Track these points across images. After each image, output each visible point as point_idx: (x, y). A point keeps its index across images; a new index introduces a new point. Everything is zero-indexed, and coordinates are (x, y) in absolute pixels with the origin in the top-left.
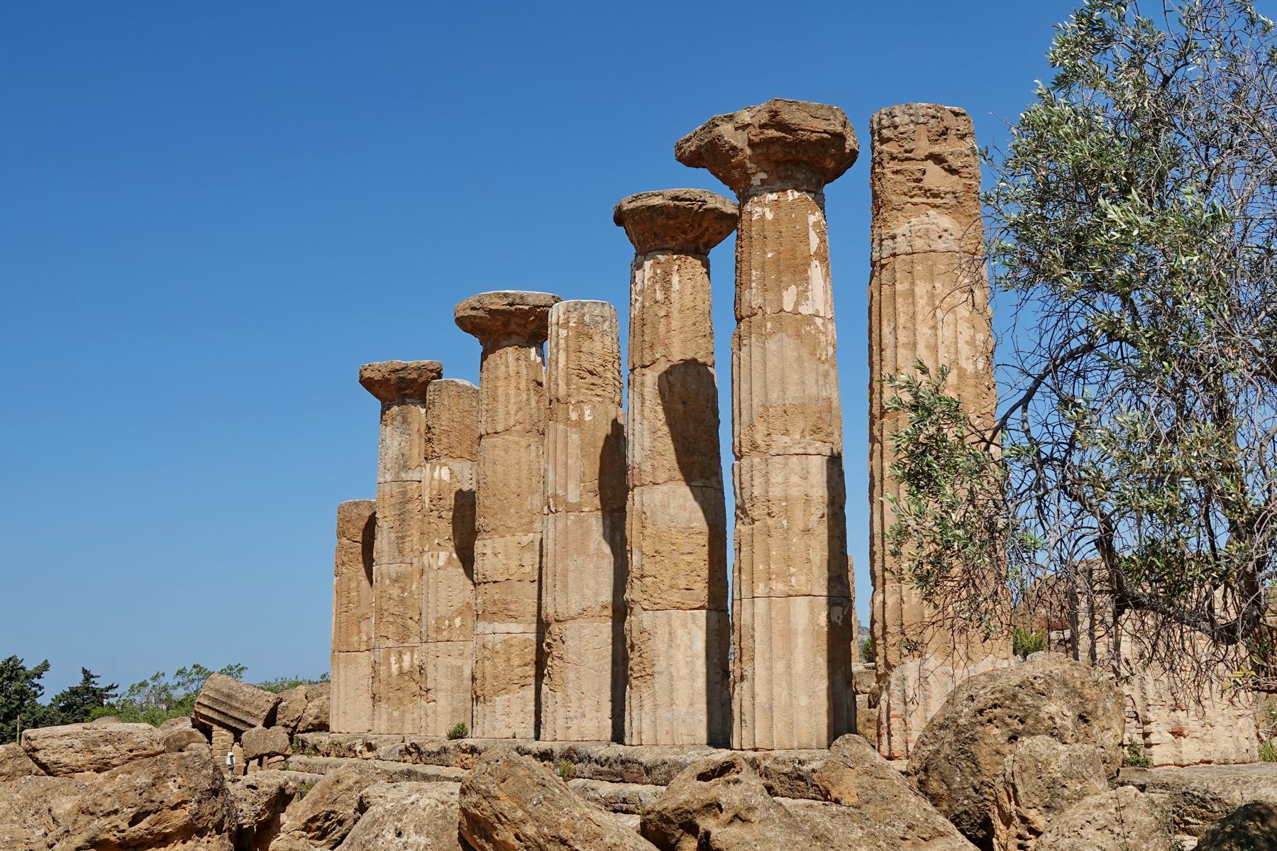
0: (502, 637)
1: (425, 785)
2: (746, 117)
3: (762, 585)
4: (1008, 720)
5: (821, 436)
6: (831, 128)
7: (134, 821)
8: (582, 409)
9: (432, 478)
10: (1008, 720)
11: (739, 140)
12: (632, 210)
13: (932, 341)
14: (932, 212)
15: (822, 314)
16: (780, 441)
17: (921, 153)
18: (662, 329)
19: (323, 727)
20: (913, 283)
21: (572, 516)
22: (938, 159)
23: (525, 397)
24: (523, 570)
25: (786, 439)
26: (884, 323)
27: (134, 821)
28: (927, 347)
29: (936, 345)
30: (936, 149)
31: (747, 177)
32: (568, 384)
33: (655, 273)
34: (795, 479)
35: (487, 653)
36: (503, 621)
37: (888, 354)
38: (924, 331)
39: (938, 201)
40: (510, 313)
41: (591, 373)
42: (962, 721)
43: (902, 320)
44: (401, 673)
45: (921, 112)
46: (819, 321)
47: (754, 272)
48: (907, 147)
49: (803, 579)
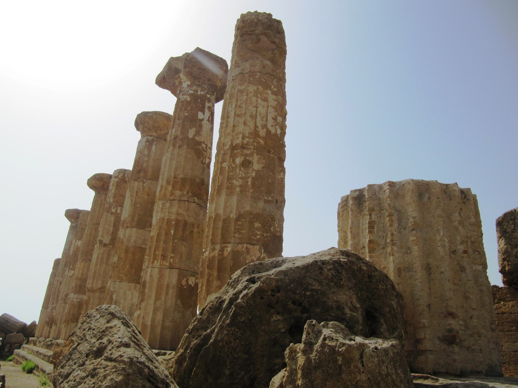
0: (78, 300)
3: (156, 262)
13: (254, 113)
16: (178, 193)
28: (251, 116)
29: (256, 115)
33: (146, 144)
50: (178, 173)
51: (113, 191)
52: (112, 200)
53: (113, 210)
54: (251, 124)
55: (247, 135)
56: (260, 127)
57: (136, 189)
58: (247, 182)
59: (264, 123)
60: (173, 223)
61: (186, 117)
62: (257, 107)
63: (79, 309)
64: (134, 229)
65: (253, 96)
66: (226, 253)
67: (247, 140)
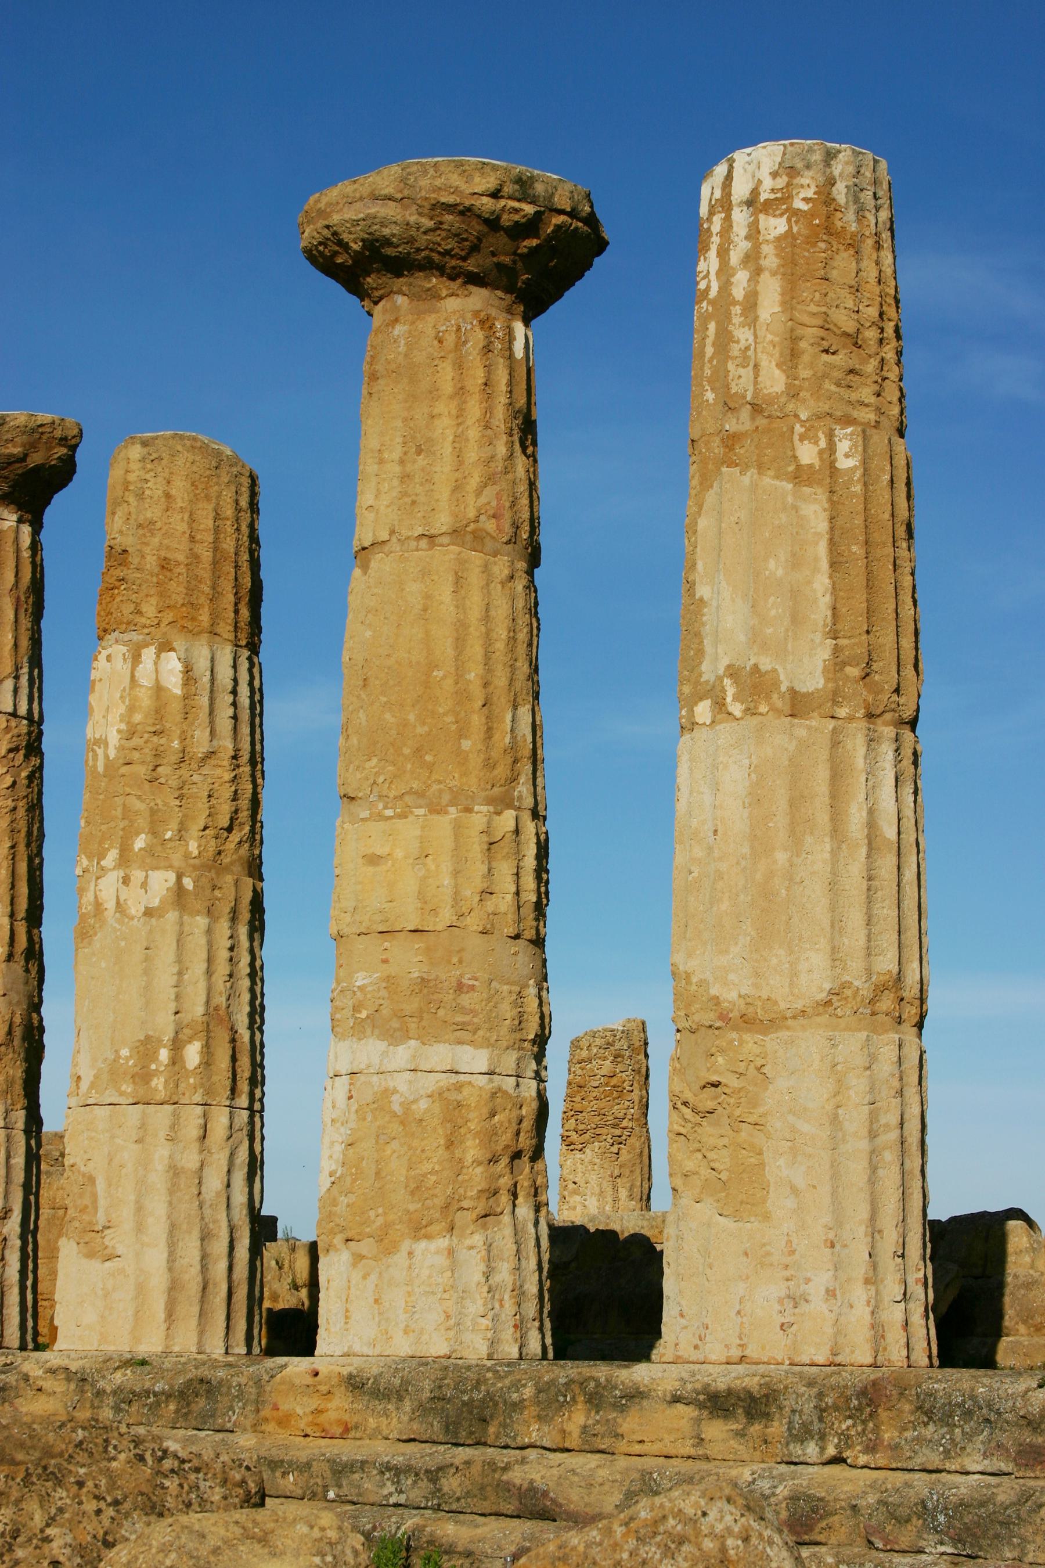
0: (431, 1083)
8: (830, 436)
21: (801, 729)
23: (502, 450)
24: (490, 905)
41: (855, 341)
51: (770, 306)
52: (774, 381)
53: (808, 454)
63: (450, 1145)
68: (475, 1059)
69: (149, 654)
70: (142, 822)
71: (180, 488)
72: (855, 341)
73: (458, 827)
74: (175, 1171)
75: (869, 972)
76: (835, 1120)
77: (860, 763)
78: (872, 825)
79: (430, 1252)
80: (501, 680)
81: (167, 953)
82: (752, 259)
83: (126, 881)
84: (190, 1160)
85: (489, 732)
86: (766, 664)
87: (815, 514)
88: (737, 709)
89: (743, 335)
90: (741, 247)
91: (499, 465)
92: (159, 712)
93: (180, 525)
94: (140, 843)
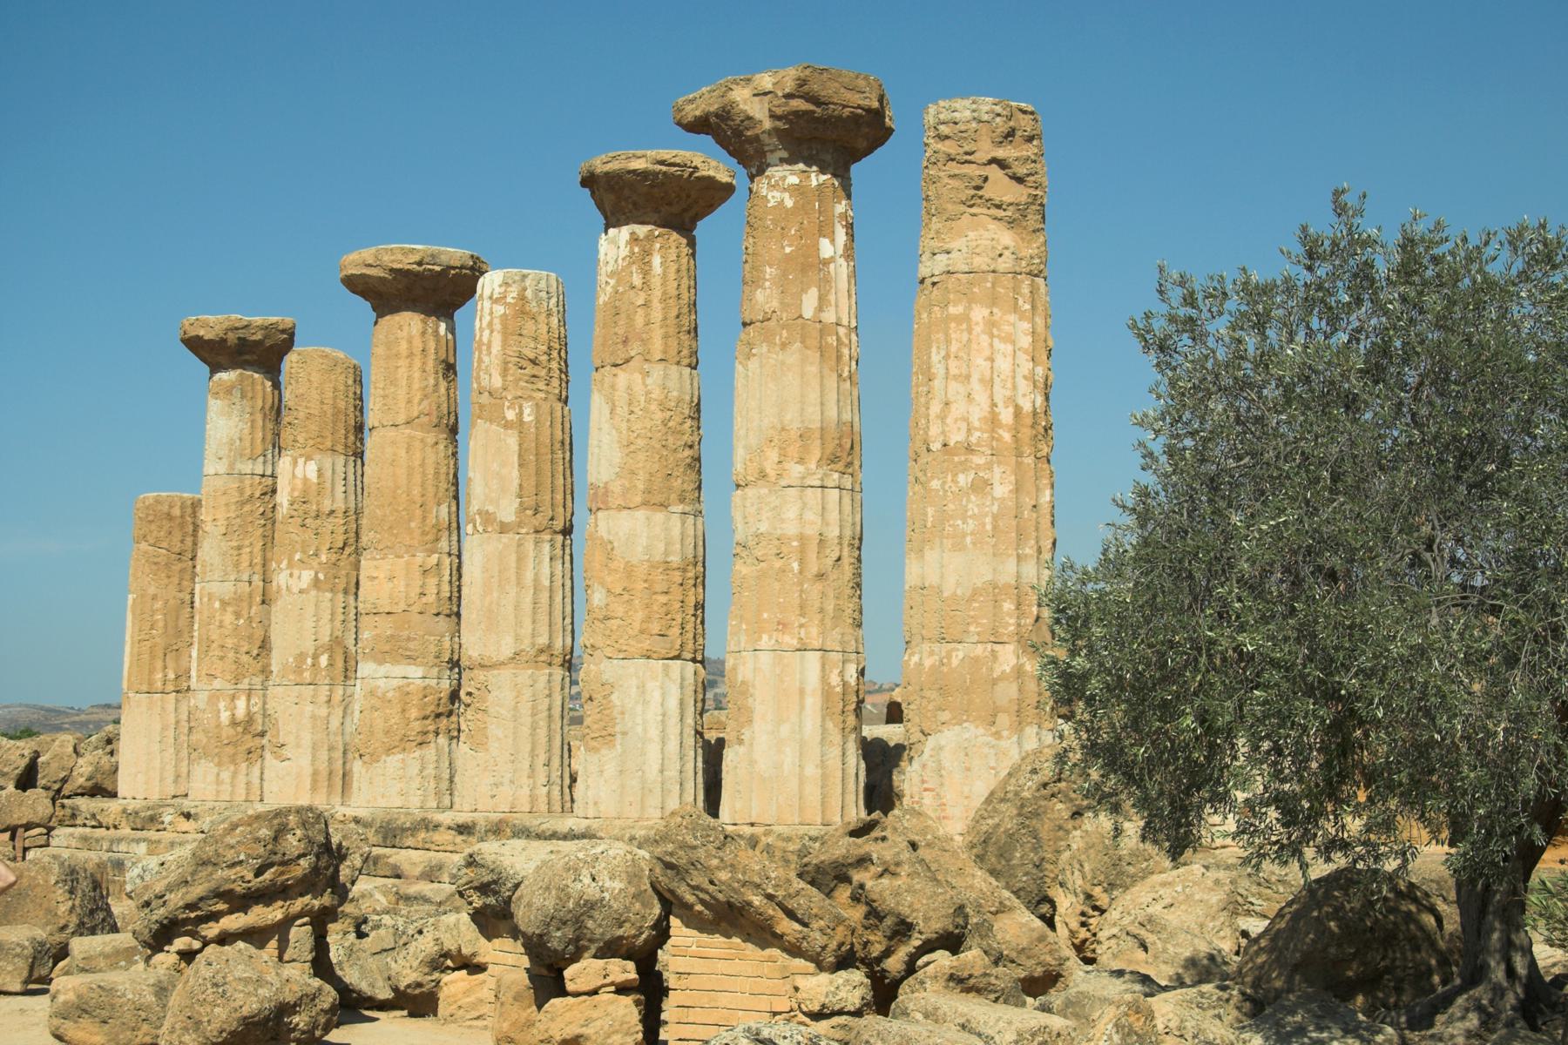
0: (395, 683)
1: (536, 844)
2: (766, 81)
3: (765, 637)
4: (1073, 795)
5: (840, 466)
6: (866, 103)
7: (259, 872)
8: (521, 407)
9: (294, 475)
10: (1073, 795)
11: (758, 111)
12: (607, 174)
13: (988, 374)
14: (993, 226)
15: (845, 322)
16: (795, 471)
17: (982, 156)
18: (639, 320)
19: (101, 790)
20: (969, 308)
21: (505, 538)
22: (1002, 164)
23: (432, 381)
24: (424, 600)
25: (800, 468)
26: (934, 350)
27: (259, 872)
28: (981, 381)
29: (992, 379)
30: (1000, 153)
31: (761, 154)
32: (505, 372)
34: (810, 516)
35: (378, 704)
36: (398, 662)
37: (937, 384)
38: (981, 362)
39: (1000, 213)
40: (417, 274)
41: (534, 362)
42: (1026, 794)
43: (953, 348)
44: (234, 723)
45: (985, 108)
46: (842, 331)
47: (768, 270)
48: (967, 148)
49: (814, 631)
50: (789, 417)
51: (496, 347)
52: (497, 382)
53: (511, 415)
54: (981, 397)
55: (977, 424)
56: (1000, 404)
57: (621, 396)
58: (984, 525)
59: (1008, 393)
60: (795, 544)
61: (788, 257)
62: (993, 361)
64: (641, 514)
65: (983, 332)
66: (955, 662)
67: (978, 434)
68: (415, 672)
69: (301, 461)
70: (298, 546)
71: (315, 377)
72: (534, 362)
73: (408, 563)
74: (314, 717)
75: (533, 645)
76: (516, 708)
77: (532, 554)
78: (536, 580)
79: (394, 761)
80: (431, 490)
81: (310, 610)
82: (490, 324)
83: (291, 575)
84: (323, 711)
85: (424, 518)
86: (491, 509)
87: (512, 441)
88: (480, 529)
89: (486, 359)
90: (487, 319)
91: (430, 389)
92: (305, 491)
93: (315, 395)
94: (297, 557)
